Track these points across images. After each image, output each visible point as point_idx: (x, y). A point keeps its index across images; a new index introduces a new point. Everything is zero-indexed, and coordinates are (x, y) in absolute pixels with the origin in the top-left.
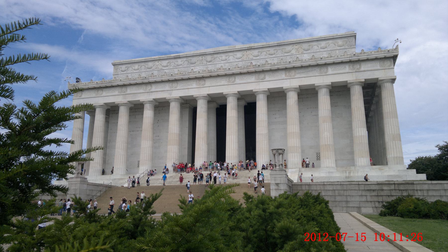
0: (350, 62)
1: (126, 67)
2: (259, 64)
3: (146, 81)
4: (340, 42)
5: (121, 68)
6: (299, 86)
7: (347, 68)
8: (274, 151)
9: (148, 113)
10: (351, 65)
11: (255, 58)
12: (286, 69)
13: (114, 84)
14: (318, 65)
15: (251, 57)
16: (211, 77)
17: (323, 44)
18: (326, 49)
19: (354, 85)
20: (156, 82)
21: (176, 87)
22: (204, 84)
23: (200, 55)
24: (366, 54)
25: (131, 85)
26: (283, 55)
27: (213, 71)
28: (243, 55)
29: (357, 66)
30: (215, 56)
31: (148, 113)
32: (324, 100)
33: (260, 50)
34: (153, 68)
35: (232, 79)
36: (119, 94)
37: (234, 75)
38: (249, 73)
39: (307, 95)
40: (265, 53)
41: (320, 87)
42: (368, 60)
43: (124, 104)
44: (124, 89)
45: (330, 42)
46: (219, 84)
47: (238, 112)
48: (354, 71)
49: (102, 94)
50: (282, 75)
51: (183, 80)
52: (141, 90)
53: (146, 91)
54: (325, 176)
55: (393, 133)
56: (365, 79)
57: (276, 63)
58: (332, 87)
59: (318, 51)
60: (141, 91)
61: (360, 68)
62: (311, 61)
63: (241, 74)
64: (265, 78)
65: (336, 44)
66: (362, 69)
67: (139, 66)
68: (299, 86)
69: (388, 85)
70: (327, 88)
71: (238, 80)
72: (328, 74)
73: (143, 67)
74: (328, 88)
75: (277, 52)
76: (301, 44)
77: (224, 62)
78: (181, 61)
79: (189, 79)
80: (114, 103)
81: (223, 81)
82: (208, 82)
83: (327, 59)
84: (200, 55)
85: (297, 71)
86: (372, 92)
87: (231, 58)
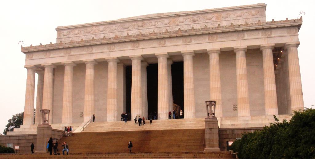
0: (263, 29)
1: (68, 32)
2: (186, 29)
4: (253, 12)
5: (63, 33)
6: (221, 48)
7: (260, 34)
8: (208, 103)
9: (90, 72)
10: (264, 31)
11: (180, 24)
12: (209, 34)
13: (60, 47)
14: (236, 31)
15: (177, 23)
17: (239, 13)
18: (241, 18)
19: (266, 48)
20: (96, 45)
21: (113, 49)
22: (138, 47)
23: (132, 21)
24: (276, 23)
25: (74, 47)
26: (204, 22)
27: (146, 35)
28: (170, 21)
29: (268, 32)
30: (146, 22)
31: (90, 72)
32: (241, 60)
33: (185, 17)
34: (91, 33)
35: (162, 42)
36: (65, 55)
37: (164, 38)
39: (228, 55)
40: (189, 20)
41: (238, 50)
42: (277, 28)
43: (68, 64)
44: (68, 51)
45: (245, 11)
46: (151, 46)
47: (168, 70)
48: (266, 37)
49: (50, 55)
50: (206, 39)
51: (119, 43)
52: (84, 51)
53: (88, 53)
54: (242, 123)
55: (297, 88)
56: (275, 44)
57: (201, 29)
58: (248, 50)
59: (235, 19)
61: (271, 34)
62: (230, 27)
63: (170, 38)
64: (191, 41)
65: (250, 14)
66: (273, 35)
67: (79, 31)
68: (221, 48)
69: (293, 49)
70: (243, 50)
71: (168, 43)
72: (244, 38)
73: (82, 32)
74: (244, 50)
75: (200, 19)
76: (220, 13)
77: (154, 27)
78: (116, 26)
79: (125, 42)
80: (60, 63)
81: (155, 44)
82: (142, 45)
83: (243, 26)
84: (132, 21)
85: (219, 36)
86: (280, 54)
87: (159, 23)
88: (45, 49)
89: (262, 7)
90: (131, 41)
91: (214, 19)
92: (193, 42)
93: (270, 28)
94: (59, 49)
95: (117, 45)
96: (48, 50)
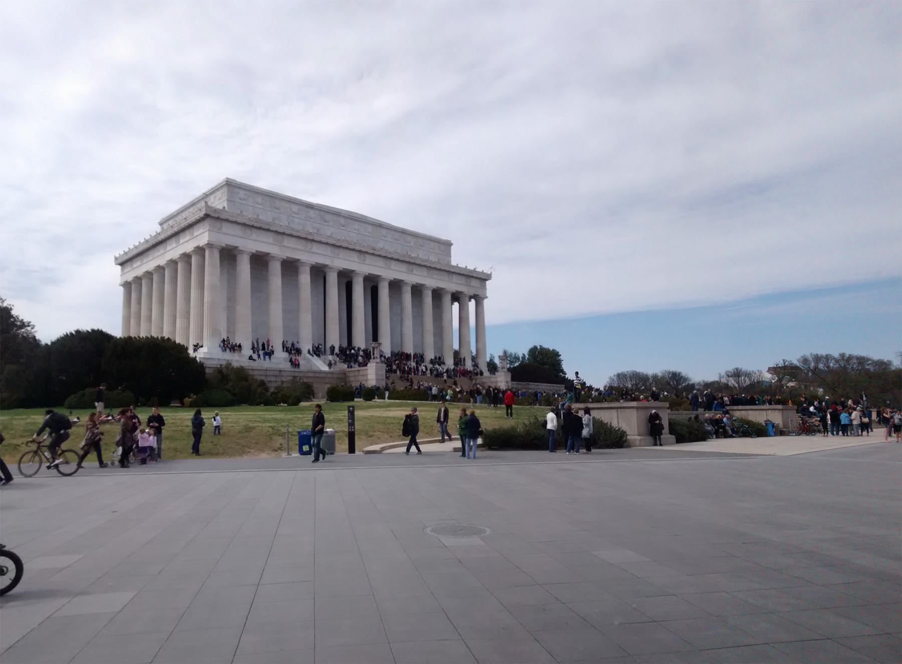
3: (310, 237)
4: (443, 247)
7: (463, 280)
16: (373, 254)
17: (432, 244)
20: (320, 242)
25: (291, 235)
35: (388, 262)
37: (392, 259)
38: (403, 261)
44: (280, 237)
50: (424, 272)
51: (347, 248)
60: (301, 247)
63: (397, 260)
64: (412, 271)
85: (437, 272)
88: (248, 222)
89: (448, 244)
90: (360, 251)
91: (412, 244)
92: (415, 272)
93: (472, 277)
94: (268, 230)
95: (341, 250)
96: (253, 227)
